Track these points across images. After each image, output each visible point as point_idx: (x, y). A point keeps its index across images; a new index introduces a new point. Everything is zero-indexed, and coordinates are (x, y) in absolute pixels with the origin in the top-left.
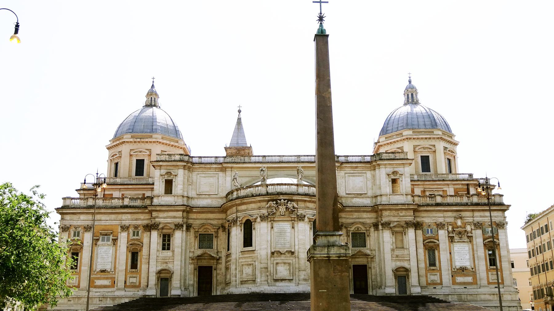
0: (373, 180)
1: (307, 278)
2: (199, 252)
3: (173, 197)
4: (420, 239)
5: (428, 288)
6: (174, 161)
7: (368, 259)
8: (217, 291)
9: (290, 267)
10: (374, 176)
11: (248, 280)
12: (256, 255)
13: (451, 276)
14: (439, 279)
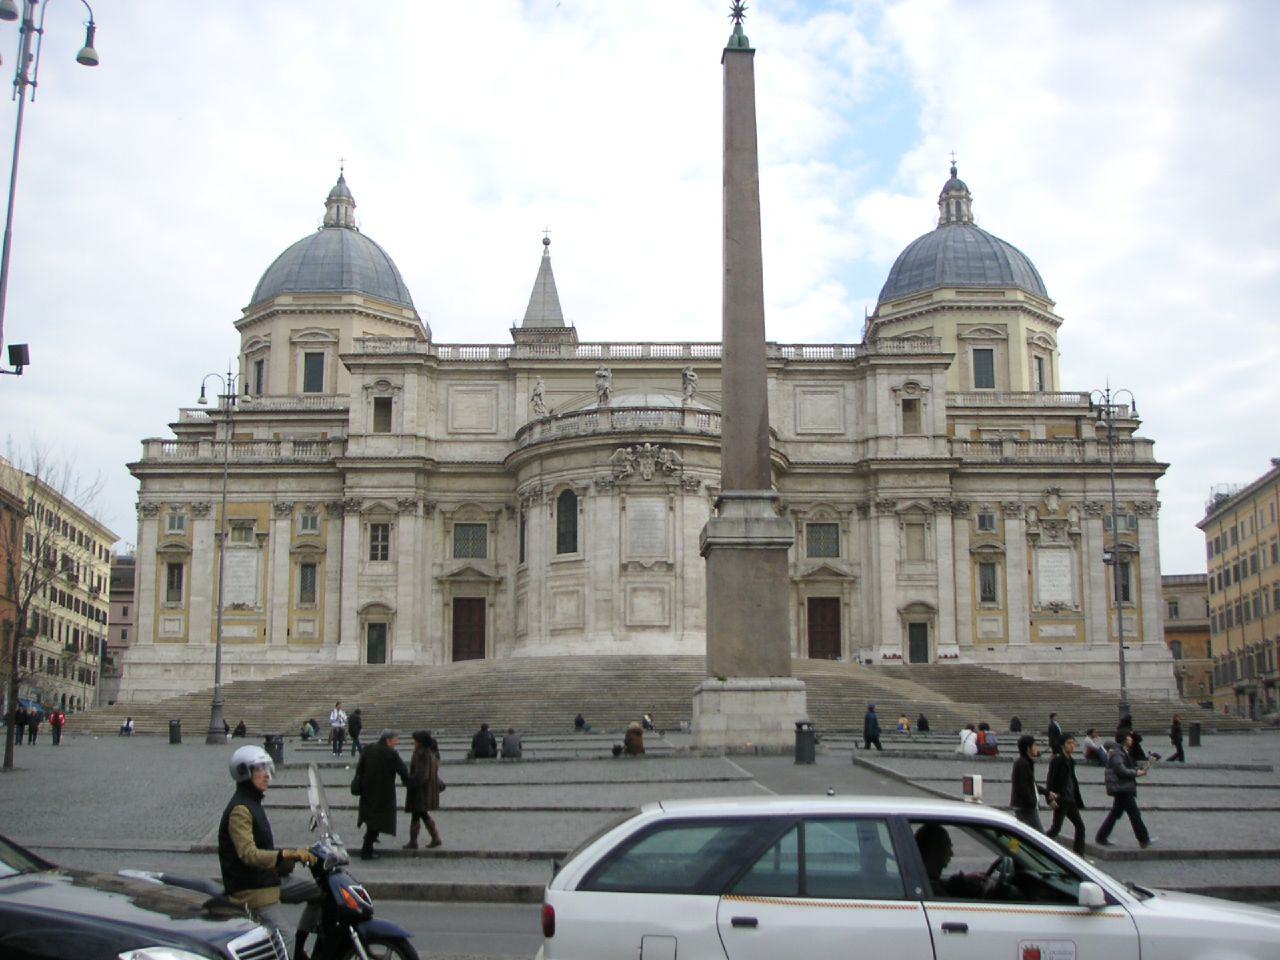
0: (860, 403)
2: (457, 565)
3: (393, 439)
4: (964, 541)
5: (976, 650)
6: (395, 355)
7: (842, 584)
8: (498, 653)
9: (663, 598)
10: (862, 395)
11: (568, 626)
12: (586, 570)
14: (1001, 629)
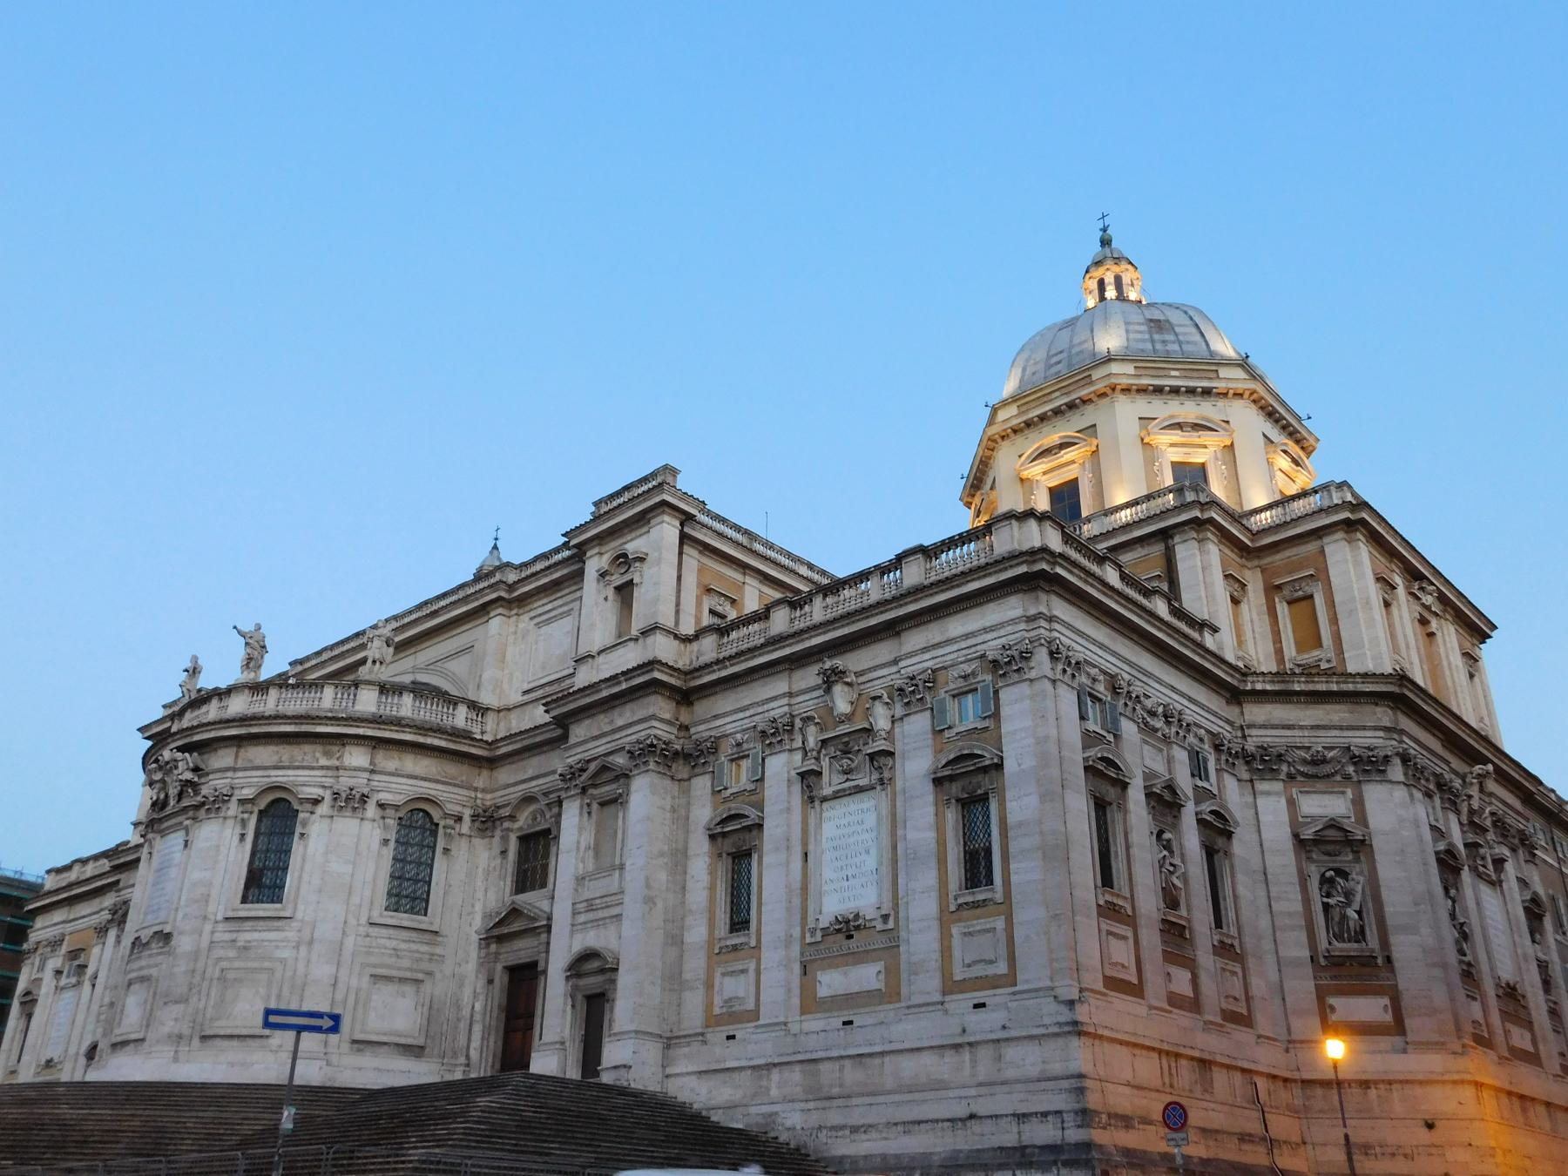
1: (186, 1031)
13: (797, 968)
